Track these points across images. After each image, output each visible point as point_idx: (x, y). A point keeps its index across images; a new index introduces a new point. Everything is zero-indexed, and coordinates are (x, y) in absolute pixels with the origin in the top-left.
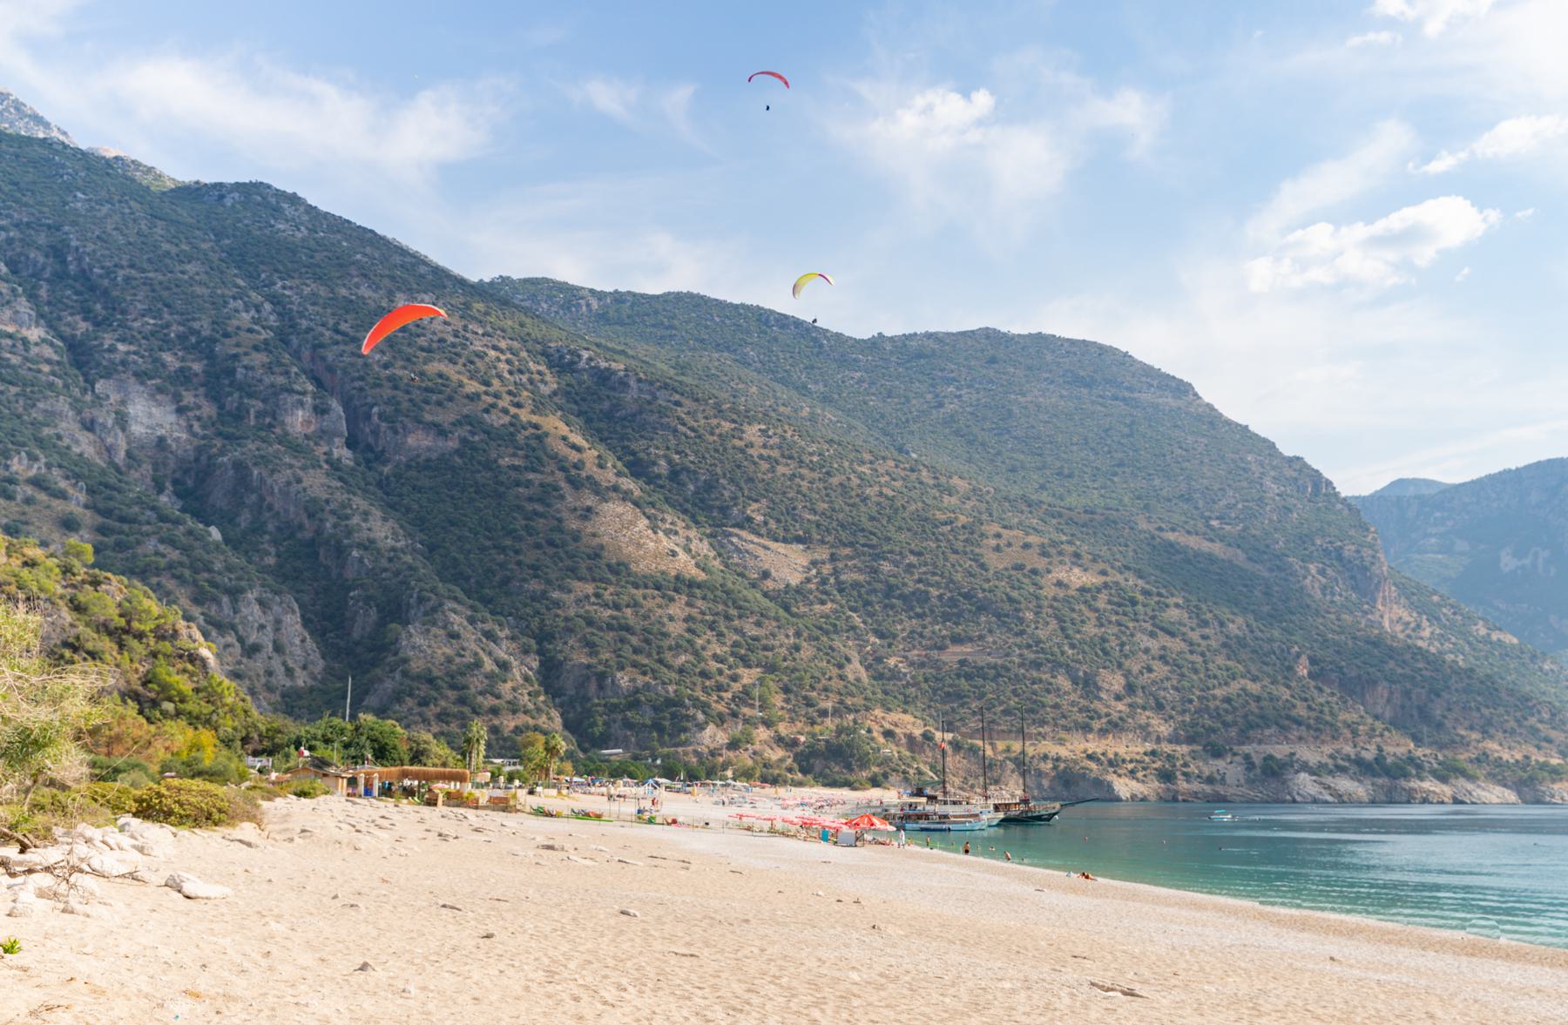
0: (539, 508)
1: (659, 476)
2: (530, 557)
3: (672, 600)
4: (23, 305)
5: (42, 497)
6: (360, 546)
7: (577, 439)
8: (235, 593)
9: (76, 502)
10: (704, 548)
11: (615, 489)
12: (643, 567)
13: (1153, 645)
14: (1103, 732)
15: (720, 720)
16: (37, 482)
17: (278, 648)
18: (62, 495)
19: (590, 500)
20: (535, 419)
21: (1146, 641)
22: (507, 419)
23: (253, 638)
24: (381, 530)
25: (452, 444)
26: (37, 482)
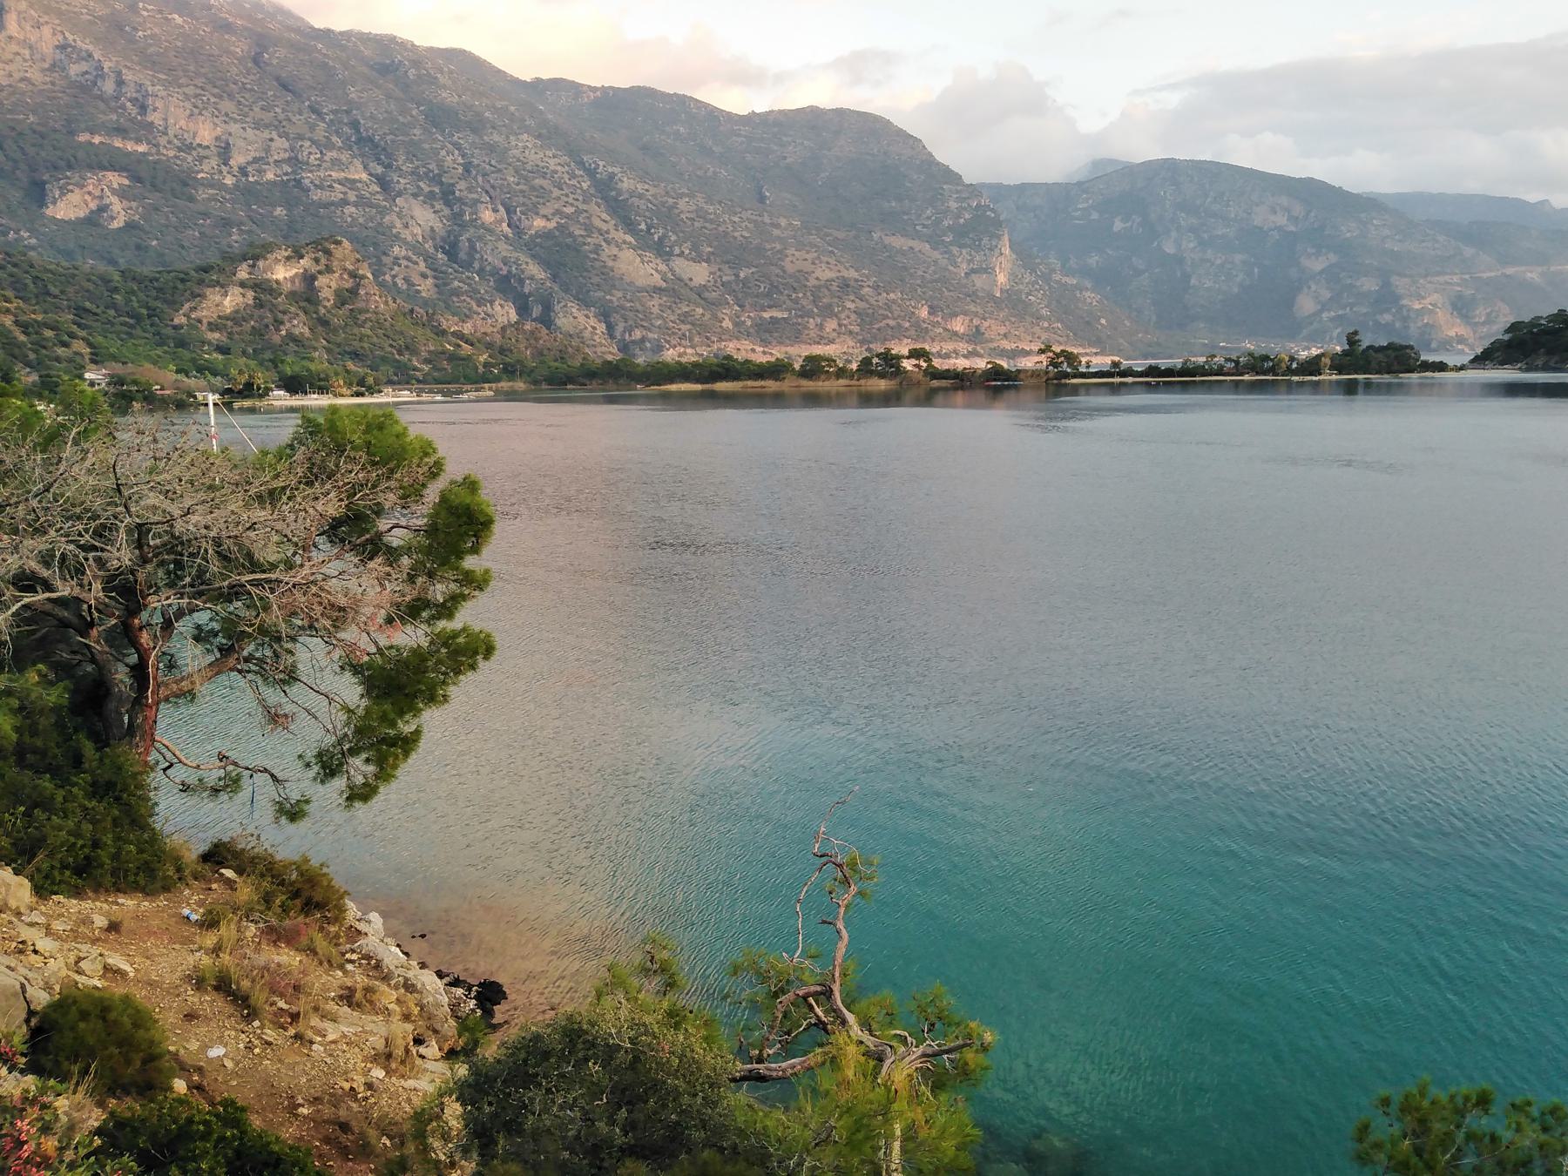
2: (596, 280)
4: (358, 163)
9: (422, 265)
10: (663, 267)
11: (625, 242)
12: (640, 283)
13: (852, 306)
16: (408, 259)
19: (615, 251)
20: (585, 207)
21: (849, 305)
25: (552, 225)
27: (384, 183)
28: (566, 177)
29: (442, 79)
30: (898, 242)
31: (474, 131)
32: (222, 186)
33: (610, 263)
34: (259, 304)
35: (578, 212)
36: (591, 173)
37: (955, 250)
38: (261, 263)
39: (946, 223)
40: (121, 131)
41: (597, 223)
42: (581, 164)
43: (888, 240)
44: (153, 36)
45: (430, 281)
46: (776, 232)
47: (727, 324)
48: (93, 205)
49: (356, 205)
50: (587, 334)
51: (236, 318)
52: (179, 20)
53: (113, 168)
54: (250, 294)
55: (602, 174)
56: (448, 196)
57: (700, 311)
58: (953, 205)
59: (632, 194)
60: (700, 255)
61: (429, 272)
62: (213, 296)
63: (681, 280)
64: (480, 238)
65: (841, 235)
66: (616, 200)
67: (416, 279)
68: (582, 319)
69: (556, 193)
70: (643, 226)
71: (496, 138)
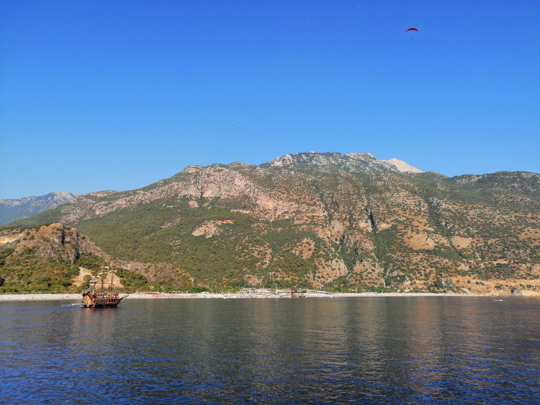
0: (400, 237)
1: (442, 225)
3: (419, 255)
5: (307, 245)
6: (361, 249)
8: (332, 260)
14: (532, 279)
17: (339, 269)
18: (310, 245)
22: (405, 219)
23: (334, 268)
25: (390, 225)
26: (307, 243)
33: (406, 240)
36: (430, 204)
59: (444, 210)
70: (444, 223)
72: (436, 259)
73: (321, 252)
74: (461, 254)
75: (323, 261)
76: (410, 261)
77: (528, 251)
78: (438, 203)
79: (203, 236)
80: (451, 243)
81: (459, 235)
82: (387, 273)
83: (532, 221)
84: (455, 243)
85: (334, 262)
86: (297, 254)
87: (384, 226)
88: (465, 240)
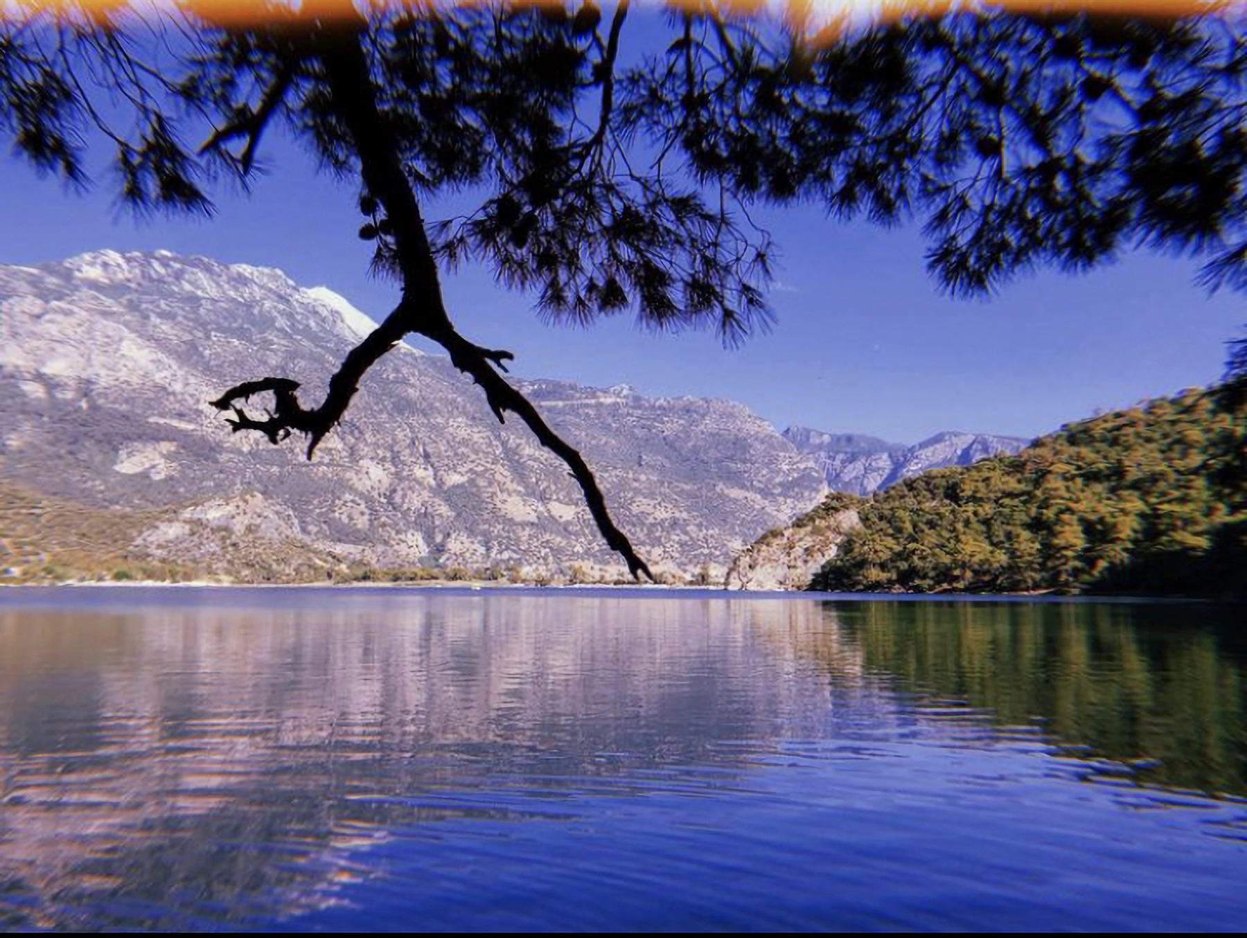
2: (486, 516)
7: (506, 473)
8: (406, 532)
9: (363, 507)
10: (541, 509)
12: (518, 519)
15: (530, 565)
16: (353, 501)
19: (505, 496)
24: (444, 509)
26: (353, 501)
27: (353, 451)
28: (484, 447)
29: (412, 381)
30: (735, 493)
31: (425, 415)
32: (240, 452)
33: (499, 505)
34: (193, 534)
35: (487, 470)
36: (504, 444)
37: (781, 499)
38: (199, 508)
39: (778, 480)
40: (181, 416)
41: (498, 477)
42: (498, 437)
43: (726, 491)
44: (217, 354)
45: (366, 517)
46: (635, 484)
47: (578, 549)
48: (147, 465)
49: (328, 465)
50: (468, 555)
51: (178, 540)
52: (236, 342)
53: (167, 439)
54: (187, 527)
55: (512, 443)
56: (395, 459)
57: (559, 539)
58: (785, 467)
59: (530, 457)
60: (571, 500)
61: (367, 511)
62: (163, 527)
63: (551, 516)
64: (410, 488)
65: (687, 487)
66: (518, 461)
67: (356, 515)
68: (467, 545)
69: (473, 457)
71: (439, 420)
72: (547, 537)
73: (383, 519)
74: (565, 530)
75: (393, 533)
76: (518, 539)
77: (645, 530)
78: (518, 445)
79: (145, 475)
80: (549, 511)
81: (558, 500)
82: (493, 555)
83: (635, 484)
84: (553, 513)
85: (409, 535)
86: (345, 519)
87: (454, 479)
88: (568, 508)
